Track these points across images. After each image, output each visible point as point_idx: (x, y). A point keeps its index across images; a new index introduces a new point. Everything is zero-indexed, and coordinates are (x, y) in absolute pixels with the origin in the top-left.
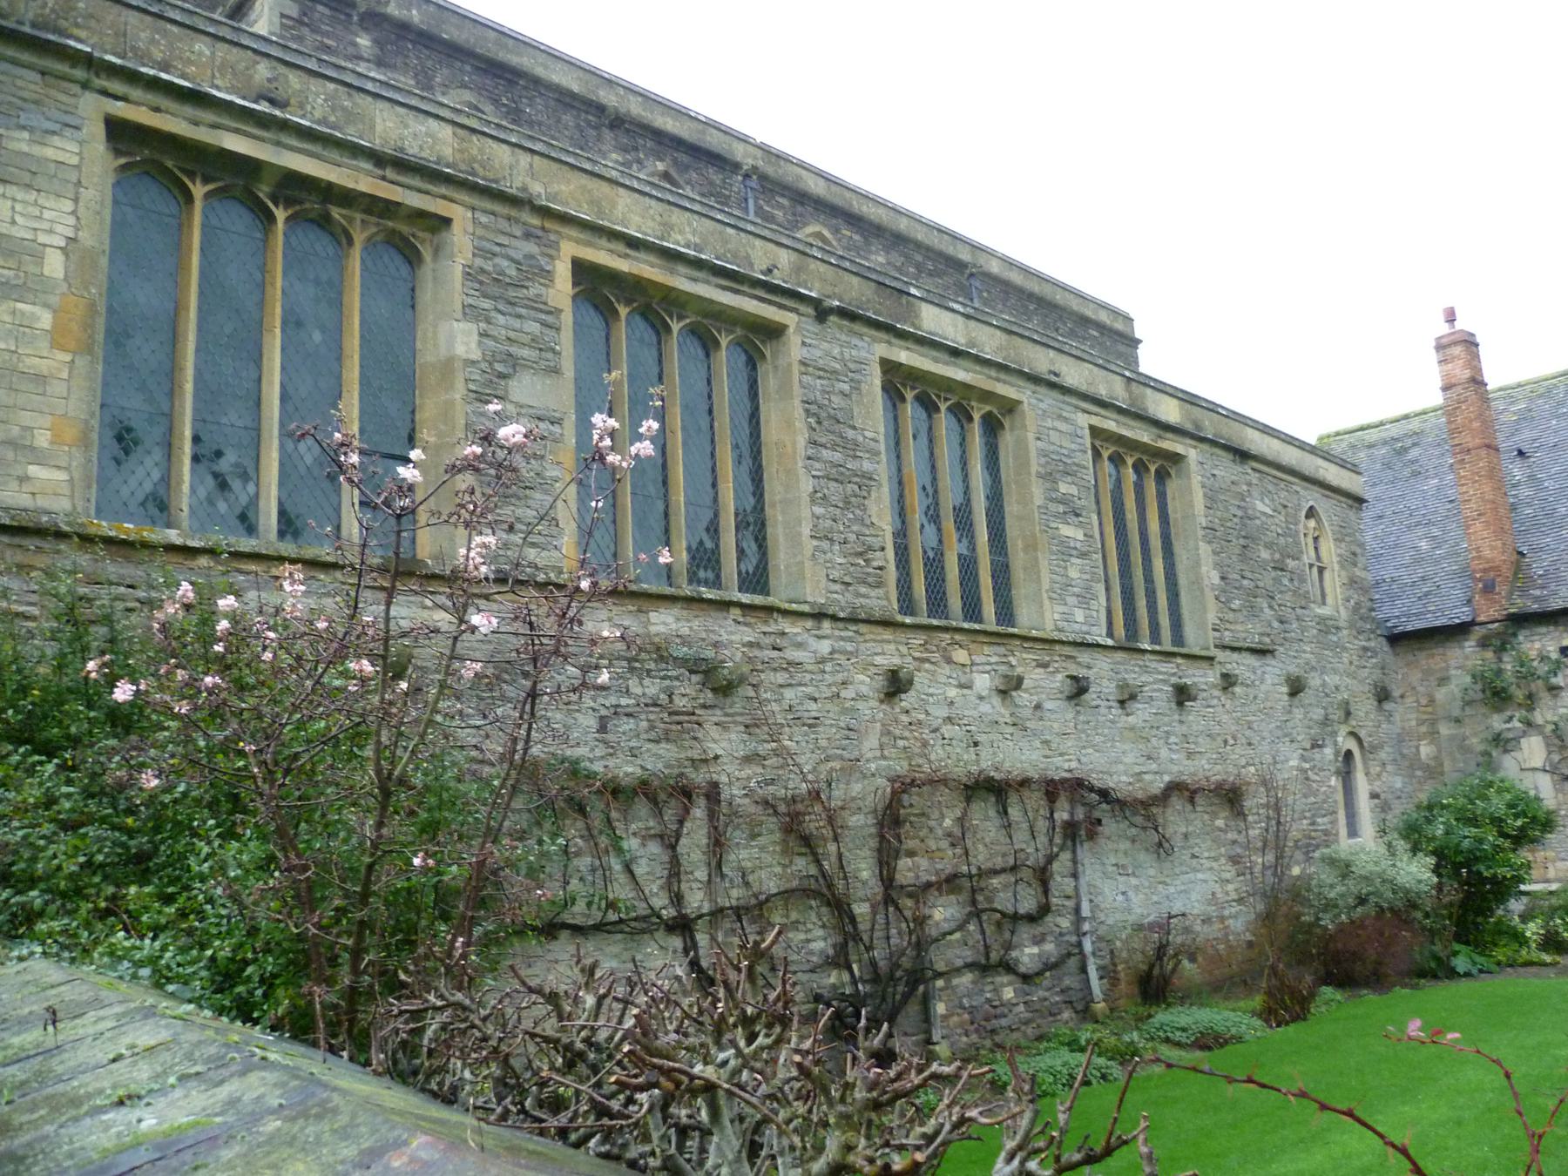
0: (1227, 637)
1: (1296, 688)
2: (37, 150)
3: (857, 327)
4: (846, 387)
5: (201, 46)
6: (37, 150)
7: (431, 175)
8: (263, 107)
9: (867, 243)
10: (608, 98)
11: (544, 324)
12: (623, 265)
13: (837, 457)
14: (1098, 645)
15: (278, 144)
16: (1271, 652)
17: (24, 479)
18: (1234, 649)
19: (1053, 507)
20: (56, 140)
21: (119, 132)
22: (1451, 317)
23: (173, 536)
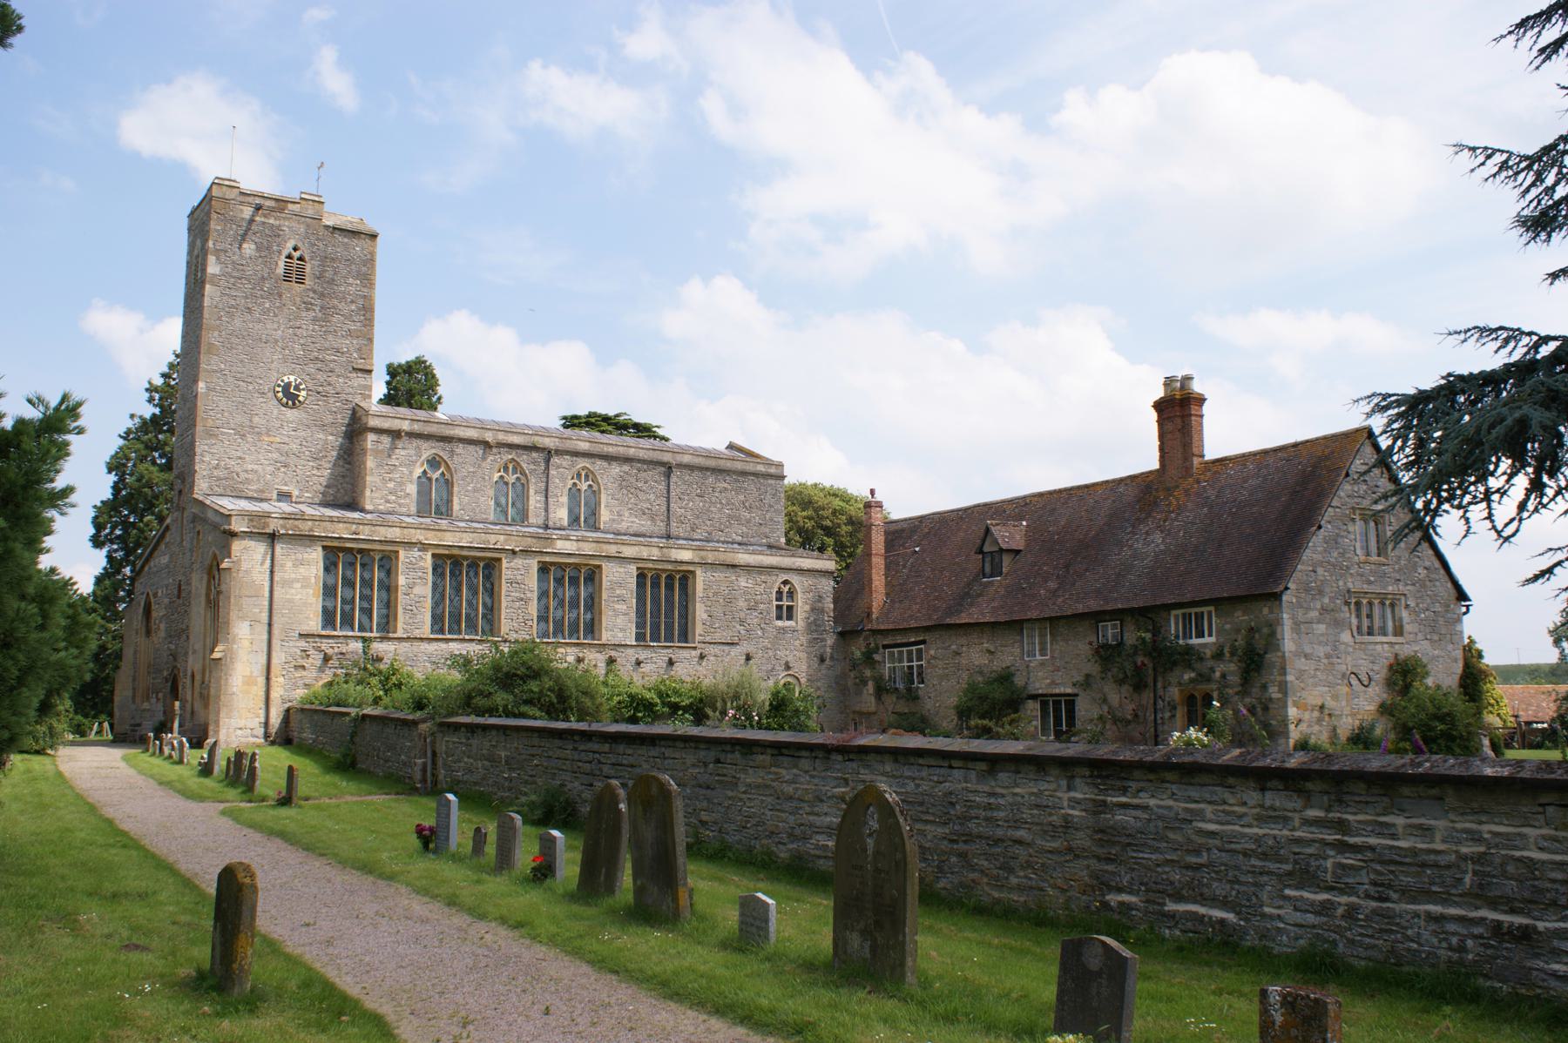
0: (708, 639)
1: (748, 658)
5: (341, 525)
8: (354, 536)
10: (489, 437)
12: (447, 552)
13: (517, 595)
14: (627, 645)
16: (737, 644)
18: (710, 643)
19: (611, 599)
22: (872, 492)
23: (335, 633)
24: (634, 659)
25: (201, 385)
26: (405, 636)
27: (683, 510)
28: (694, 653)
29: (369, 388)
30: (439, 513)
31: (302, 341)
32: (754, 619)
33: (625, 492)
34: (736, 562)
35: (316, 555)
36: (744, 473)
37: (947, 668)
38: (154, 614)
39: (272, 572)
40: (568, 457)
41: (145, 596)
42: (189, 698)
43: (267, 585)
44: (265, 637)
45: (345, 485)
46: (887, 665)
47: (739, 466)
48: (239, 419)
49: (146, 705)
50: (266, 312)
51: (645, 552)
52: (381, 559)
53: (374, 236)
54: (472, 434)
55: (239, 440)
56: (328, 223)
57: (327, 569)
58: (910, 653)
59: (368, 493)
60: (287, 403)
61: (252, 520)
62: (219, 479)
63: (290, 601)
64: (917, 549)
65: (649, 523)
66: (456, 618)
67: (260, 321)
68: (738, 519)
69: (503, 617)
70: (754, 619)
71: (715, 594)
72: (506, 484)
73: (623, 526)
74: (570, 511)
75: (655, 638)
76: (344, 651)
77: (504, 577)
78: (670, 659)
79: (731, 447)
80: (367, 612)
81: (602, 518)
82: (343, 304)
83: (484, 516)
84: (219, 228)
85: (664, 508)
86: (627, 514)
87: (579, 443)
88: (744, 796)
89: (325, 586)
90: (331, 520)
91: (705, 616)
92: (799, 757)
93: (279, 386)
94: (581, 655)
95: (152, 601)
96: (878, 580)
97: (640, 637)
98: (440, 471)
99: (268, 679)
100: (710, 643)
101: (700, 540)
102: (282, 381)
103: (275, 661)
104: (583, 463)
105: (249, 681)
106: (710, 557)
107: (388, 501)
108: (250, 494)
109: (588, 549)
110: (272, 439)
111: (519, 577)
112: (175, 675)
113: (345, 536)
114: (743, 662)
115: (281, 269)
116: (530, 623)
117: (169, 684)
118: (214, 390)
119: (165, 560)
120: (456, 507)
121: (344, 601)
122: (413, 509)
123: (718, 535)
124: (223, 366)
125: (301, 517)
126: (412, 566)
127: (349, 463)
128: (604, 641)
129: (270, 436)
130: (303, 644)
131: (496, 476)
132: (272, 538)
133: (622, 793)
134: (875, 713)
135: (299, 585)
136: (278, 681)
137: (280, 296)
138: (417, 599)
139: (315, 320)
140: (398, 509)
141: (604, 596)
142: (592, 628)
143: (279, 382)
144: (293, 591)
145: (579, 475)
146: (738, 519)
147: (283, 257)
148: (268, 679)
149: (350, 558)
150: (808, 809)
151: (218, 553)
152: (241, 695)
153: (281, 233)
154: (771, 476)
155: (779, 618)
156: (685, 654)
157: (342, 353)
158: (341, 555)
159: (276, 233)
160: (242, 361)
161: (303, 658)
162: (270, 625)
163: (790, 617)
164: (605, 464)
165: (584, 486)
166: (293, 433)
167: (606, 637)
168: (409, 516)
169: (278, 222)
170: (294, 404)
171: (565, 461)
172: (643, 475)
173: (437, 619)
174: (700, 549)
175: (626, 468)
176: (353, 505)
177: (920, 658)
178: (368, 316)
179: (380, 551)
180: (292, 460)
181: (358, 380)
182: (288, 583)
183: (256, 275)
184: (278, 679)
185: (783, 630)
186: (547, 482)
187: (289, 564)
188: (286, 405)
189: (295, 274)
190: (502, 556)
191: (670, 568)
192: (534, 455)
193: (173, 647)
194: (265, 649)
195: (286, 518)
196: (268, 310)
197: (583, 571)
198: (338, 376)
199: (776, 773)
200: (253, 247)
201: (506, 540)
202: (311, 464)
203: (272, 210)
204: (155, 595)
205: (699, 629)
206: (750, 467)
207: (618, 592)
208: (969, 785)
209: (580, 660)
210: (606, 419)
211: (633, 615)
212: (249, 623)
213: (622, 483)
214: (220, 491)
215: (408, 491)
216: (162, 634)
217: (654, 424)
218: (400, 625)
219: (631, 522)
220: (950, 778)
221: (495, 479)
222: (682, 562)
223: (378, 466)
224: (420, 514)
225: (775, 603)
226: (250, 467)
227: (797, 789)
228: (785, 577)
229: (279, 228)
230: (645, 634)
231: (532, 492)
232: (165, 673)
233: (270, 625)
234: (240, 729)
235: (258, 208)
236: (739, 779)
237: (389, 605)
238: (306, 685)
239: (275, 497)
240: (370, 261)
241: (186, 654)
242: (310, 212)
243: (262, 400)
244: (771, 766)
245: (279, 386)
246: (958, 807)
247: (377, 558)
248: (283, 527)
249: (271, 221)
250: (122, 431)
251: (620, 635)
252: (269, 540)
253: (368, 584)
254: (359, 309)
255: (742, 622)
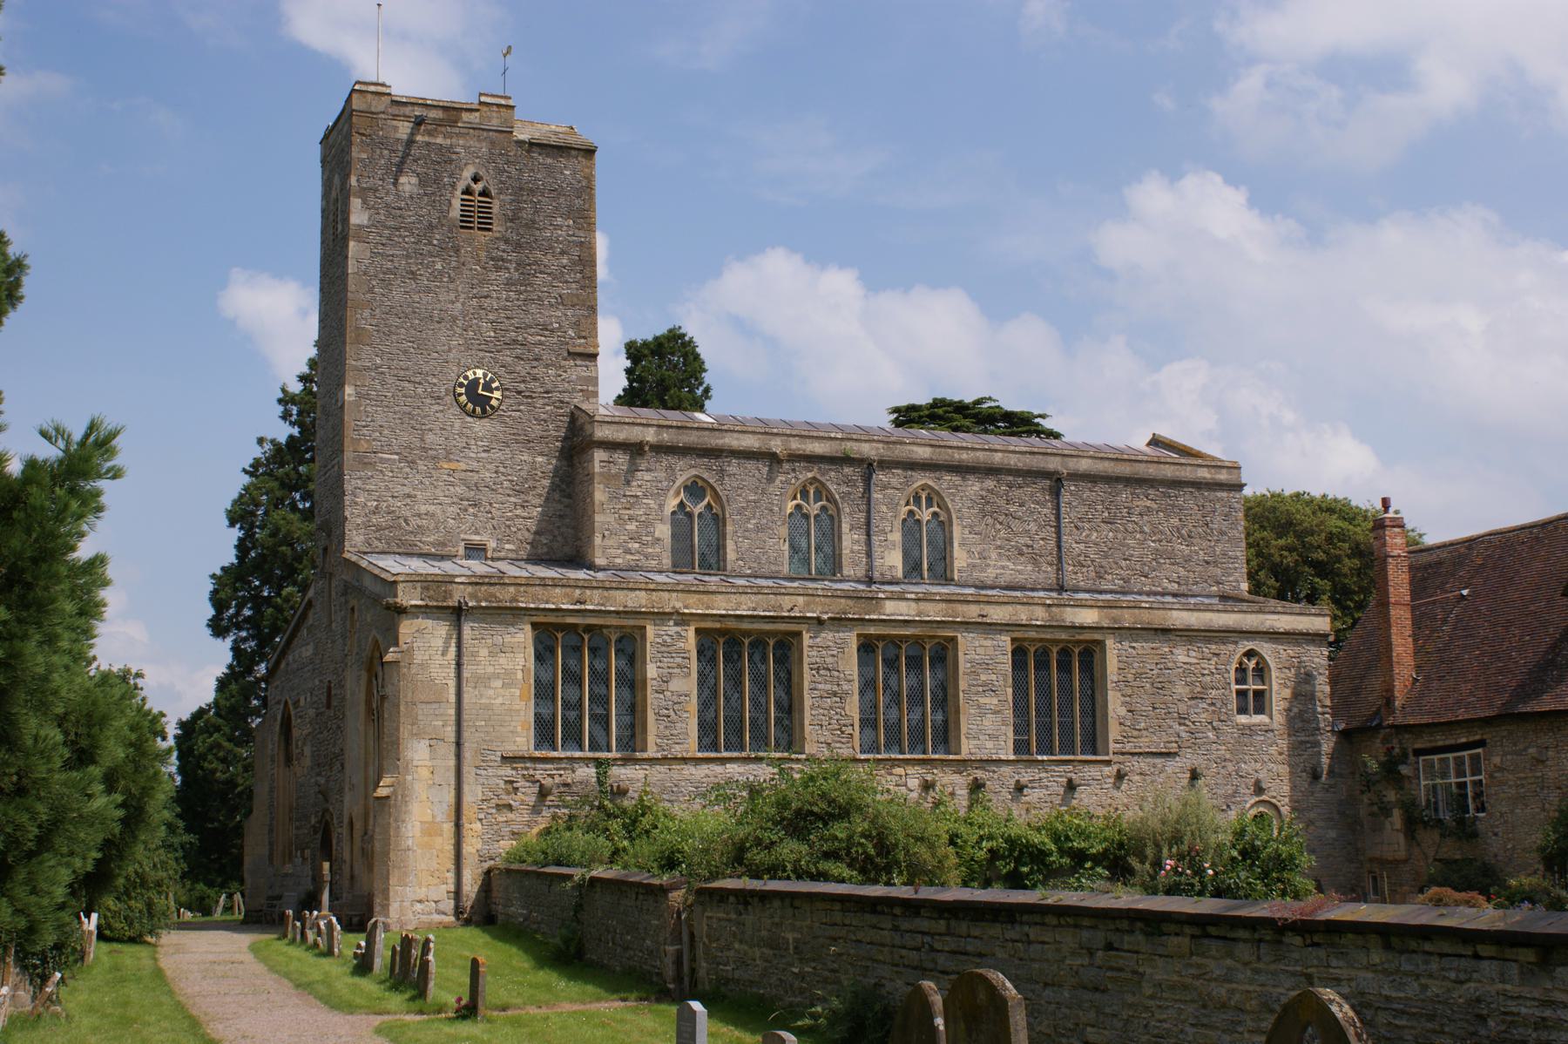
0: (1128, 747)
1: (1195, 775)
2: (513, 640)
3: (843, 623)
4: (835, 653)
5: (558, 590)
6: (513, 640)
7: (636, 614)
9: (964, 479)
10: (776, 446)
11: (683, 658)
12: (718, 625)
13: (828, 687)
15: (584, 616)
17: (515, 742)
18: (1133, 754)
20: (518, 635)
21: (535, 626)
22: (1386, 503)
24: (1012, 782)
25: (349, 390)
26: (659, 755)
27: (1082, 546)
28: (1107, 770)
29: (594, 381)
30: (706, 567)
31: (491, 317)
32: (1201, 713)
33: (990, 521)
34: (1169, 624)
35: (522, 637)
36: (1177, 484)
37: (1523, 786)
38: (296, 733)
39: (459, 665)
40: (899, 471)
41: (282, 707)
42: (347, 856)
43: (452, 684)
44: (452, 763)
45: (563, 529)
46: (1423, 783)
47: (1169, 472)
48: (405, 438)
49: (289, 868)
50: (436, 276)
51: (1023, 614)
52: (619, 641)
53: (590, 152)
54: (750, 442)
55: (408, 470)
56: (521, 137)
57: (539, 658)
58: (1459, 762)
59: (598, 540)
60: (474, 411)
61: (427, 589)
62: (379, 528)
63: (488, 707)
64: (1465, 592)
65: (1029, 568)
66: (736, 727)
67: (428, 290)
68: (1171, 556)
69: (807, 722)
70: (1201, 713)
71: (1137, 676)
72: (806, 517)
73: (990, 574)
74: (906, 555)
75: (1046, 748)
76: (569, 781)
77: (806, 660)
78: (1070, 781)
79: (1155, 442)
80: (602, 721)
81: (957, 564)
82: (549, 257)
83: (773, 568)
84: (364, 156)
85: (1053, 543)
86: (994, 556)
87: (915, 448)
88: (1151, 1003)
89: (538, 682)
90: (543, 583)
91: (1122, 711)
92: (1234, 940)
93: (461, 385)
94: (929, 777)
95: (292, 713)
96: (1402, 644)
97: (1021, 747)
98: (705, 502)
99: (458, 826)
100: (1133, 754)
101: (1111, 592)
102: (466, 378)
103: (468, 798)
104: (921, 479)
105: (430, 830)
106: (1128, 618)
107: (628, 551)
108: (426, 549)
109: (934, 612)
110: (453, 466)
111: (829, 660)
112: (327, 824)
113: (564, 607)
114: (1186, 782)
115: (456, 212)
116: (849, 730)
117: (319, 836)
118: (367, 396)
119: (307, 652)
120: (731, 555)
121: (567, 705)
122: (667, 562)
123: (1138, 583)
124: (378, 361)
125: (500, 580)
126: (666, 648)
127: (569, 496)
128: (964, 755)
129: (450, 460)
130: (507, 771)
131: (790, 506)
132: (457, 614)
133: (937, 1000)
134: (1405, 861)
135: (498, 683)
136: (473, 828)
137: (457, 250)
138: (675, 699)
139: (509, 283)
140: (644, 562)
141: (963, 685)
142: (946, 735)
143: (461, 380)
144: (491, 692)
145: (917, 499)
146: (1171, 556)
147: (458, 193)
148: (458, 826)
149: (573, 640)
150: (1250, 1024)
151: (380, 639)
152: (419, 851)
153: (454, 157)
154: (1220, 486)
155: (1242, 710)
156: (1093, 771)
157: (552, 331)
158: (560, 636)
159: (446, 158)
160: (405, 352)
161: (508, 793)
162: (458, 744)
163: (1259, 710)
164: (957, 479)
165: (925, 515)
166: (484, 455)
167: (967, 748)
168: (660, 572)
169: (448, 142)
170: (484, 411)
171: (895, 478)
172: (1017, 493)
173: (707, 730)
174: (1109, 606)
175: (990, 483)
176: (577, 558)
177: (1476, 771)
178: (587, 271)
179: (617, 627)
180: (485, 496)
181: (576, 371)
182: (483, 681)
183: (420, 222)
184: (473, 826)
185: (1249, 730)
186: (869, 512)
187: (484, 652)
188: (472, 414)
189: (477, 217)
190: (803, 628)
191: (1063, 636)
192: (847, 470)
193: (322, 781)
194: (453, 781)
195: (477, 582)
196: (441, 273)
197: (927, 647)
198: (547, 366)
199: (1199, 966)
200: (414, 180)
201: (807, 604)
202: (512, 499)
203: (439, 123)
204: (296, 704)
205: (1114, 732)
206: (1187, 474)
207: (983, 677)
208: (1508, 987)
209: (927, 786)
210: (961, 408)
211: (1009, 713)
212: (427, 742)
213: (986, 508)
214: (381, 546)
215: (657, 535)
216: (307, 762)
217: (1036, 413)
218: (651, 739)
219: (1001, 568)
220: (1475, 975)
221: (789, 511)
222: (1082, 628)
223: (611, 499)
224: (677, 568)
225: (1235, 687)
226: (423, 509)
227: (1232, 992)
228: (1249, 645)
229: (450, 149)
230: (1028, 743)
231: (845, 527)
232: (313, 821)
233: (458, 744)
234: (420, 901)
235: (419, 122)
236: (1142, 975)
237: (635, 711)
238: (513, 833)
239: (461, 551)
240: (586, 190)
241: (341, 791)
242: (495, 123)
243: (436, 407)
244: (1192, 954)
245: (461, 385)
246: (1491, 1023)
247: (614, 638)
248: (473, 596)
249: (439, 140)
250: (247, 464)
251: (990, 744)
252: (454, 617)
253: (600, 678)
254: (574, 264)
255: (1182, 720)
